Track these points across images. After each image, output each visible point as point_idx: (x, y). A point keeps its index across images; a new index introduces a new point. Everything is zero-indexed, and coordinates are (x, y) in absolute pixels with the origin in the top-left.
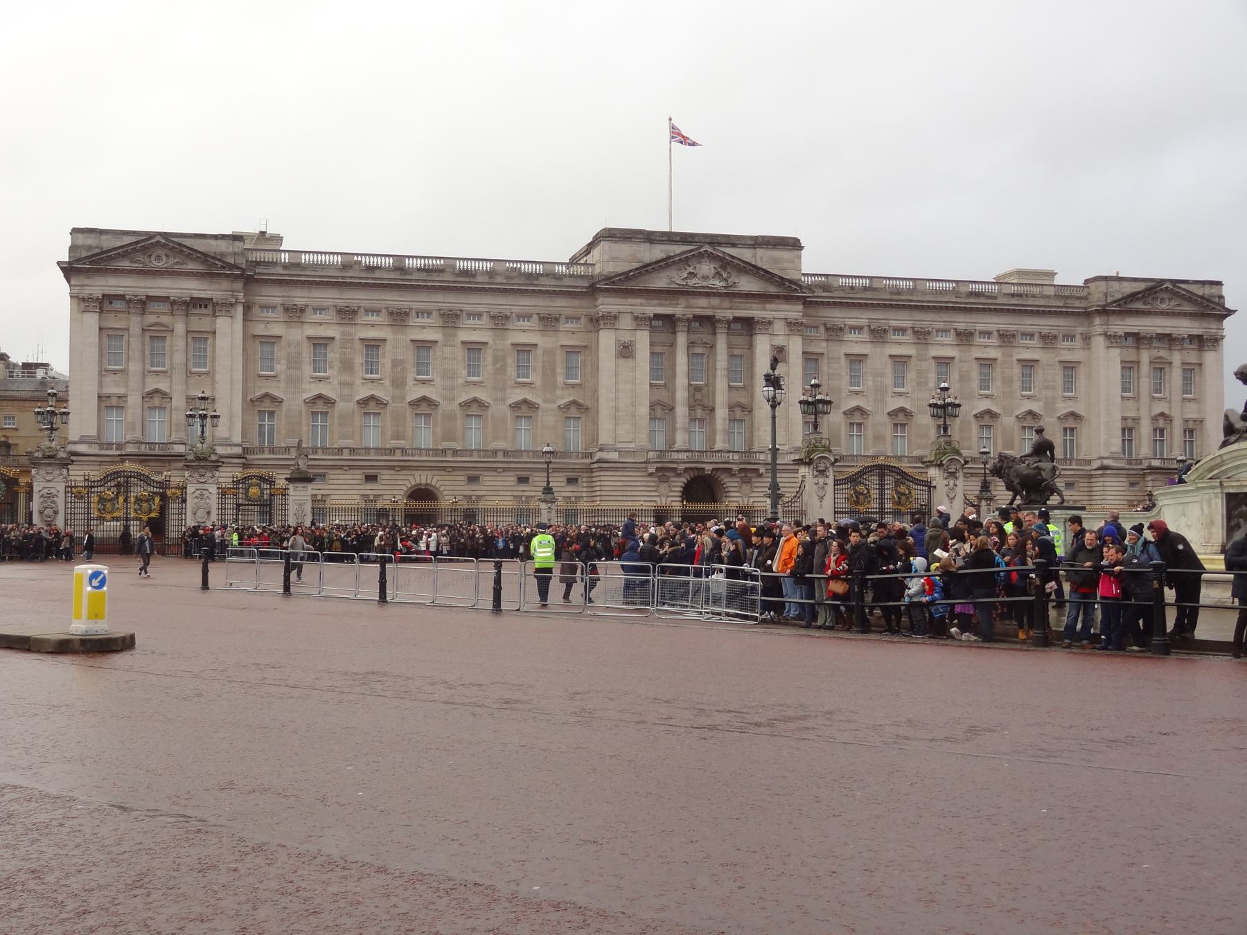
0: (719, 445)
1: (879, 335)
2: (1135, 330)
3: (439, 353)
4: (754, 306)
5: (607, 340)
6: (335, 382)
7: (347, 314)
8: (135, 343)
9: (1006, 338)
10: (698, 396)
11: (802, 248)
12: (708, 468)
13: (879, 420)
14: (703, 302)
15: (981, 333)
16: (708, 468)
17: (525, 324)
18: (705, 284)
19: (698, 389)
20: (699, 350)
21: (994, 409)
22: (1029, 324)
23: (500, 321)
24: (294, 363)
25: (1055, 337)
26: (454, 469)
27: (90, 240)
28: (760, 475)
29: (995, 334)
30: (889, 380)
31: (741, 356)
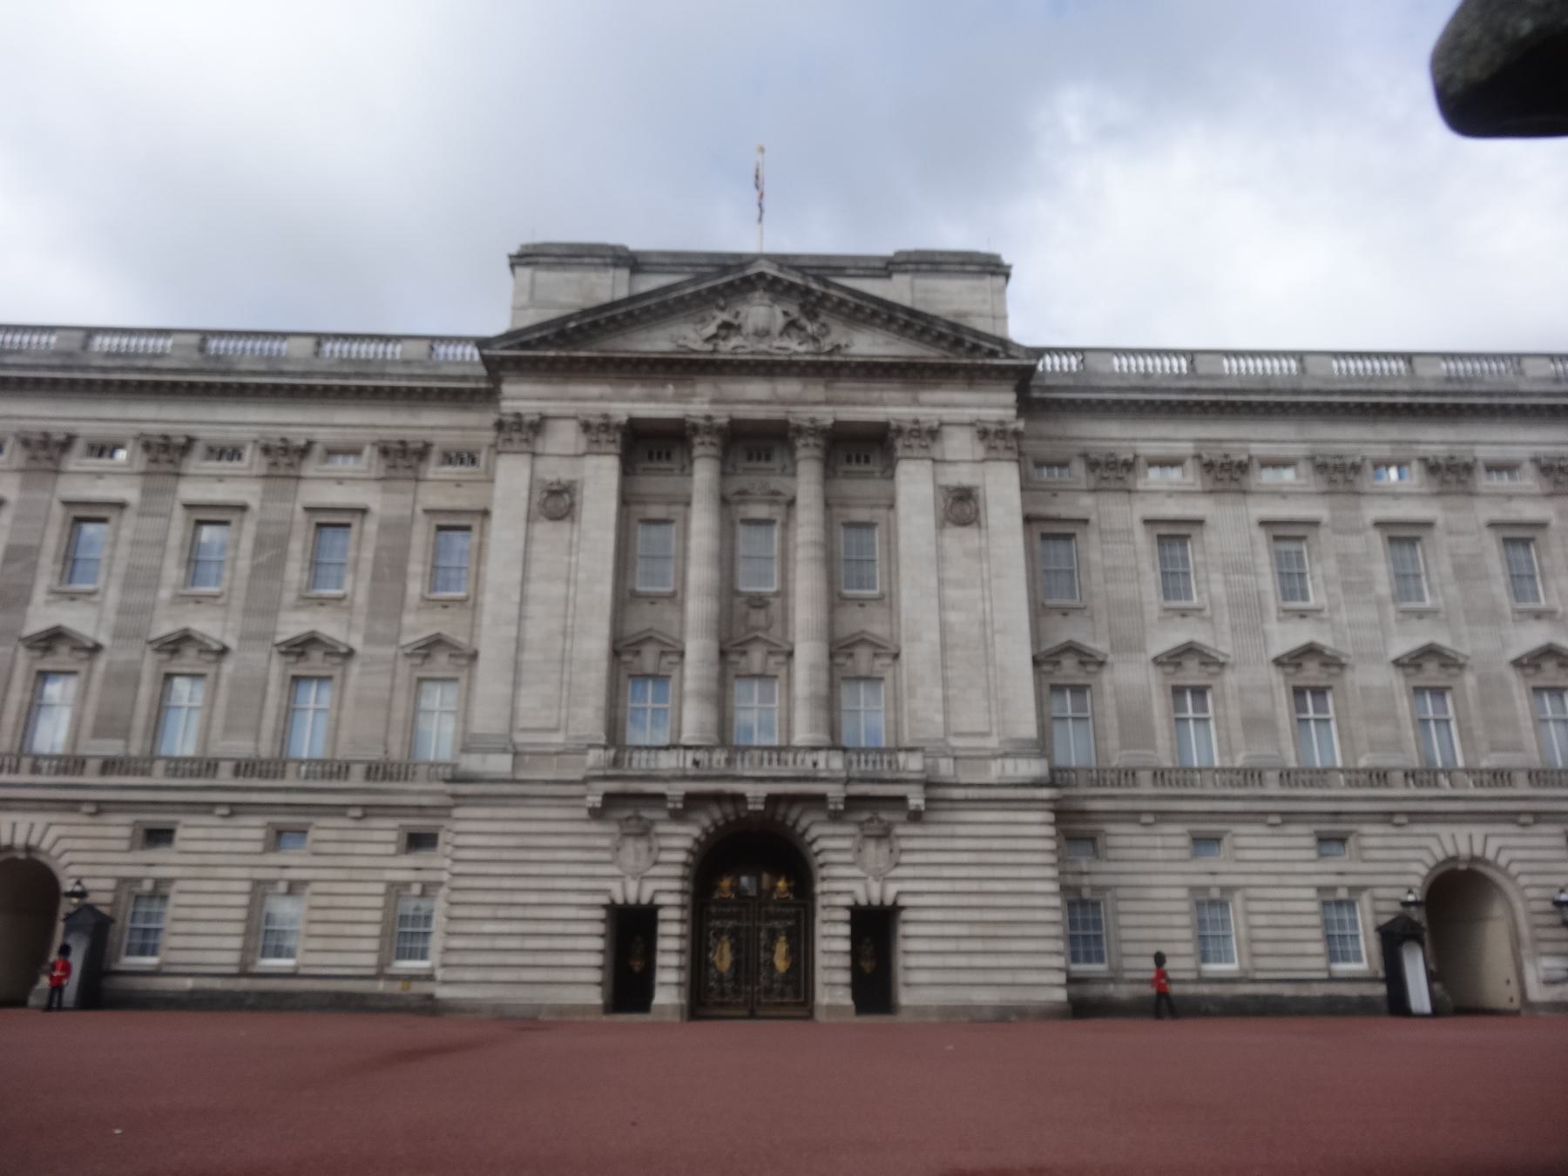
1: (1227, 474)
3: (126, 533)
4: (886, 395)
5: (512, 479)
10: (757, 618)
11: (1007, 276)
12: (755, 792)
13: (1251, 682)
14: (757, 389)
15: (1494, 468)
16: (755, 792)
18: (763, 346)
19: (759, 602)
26: (101, 808)
28: (916, 817)
29: (1528, 468)
30: (1267, 582)
31: (870, 525)
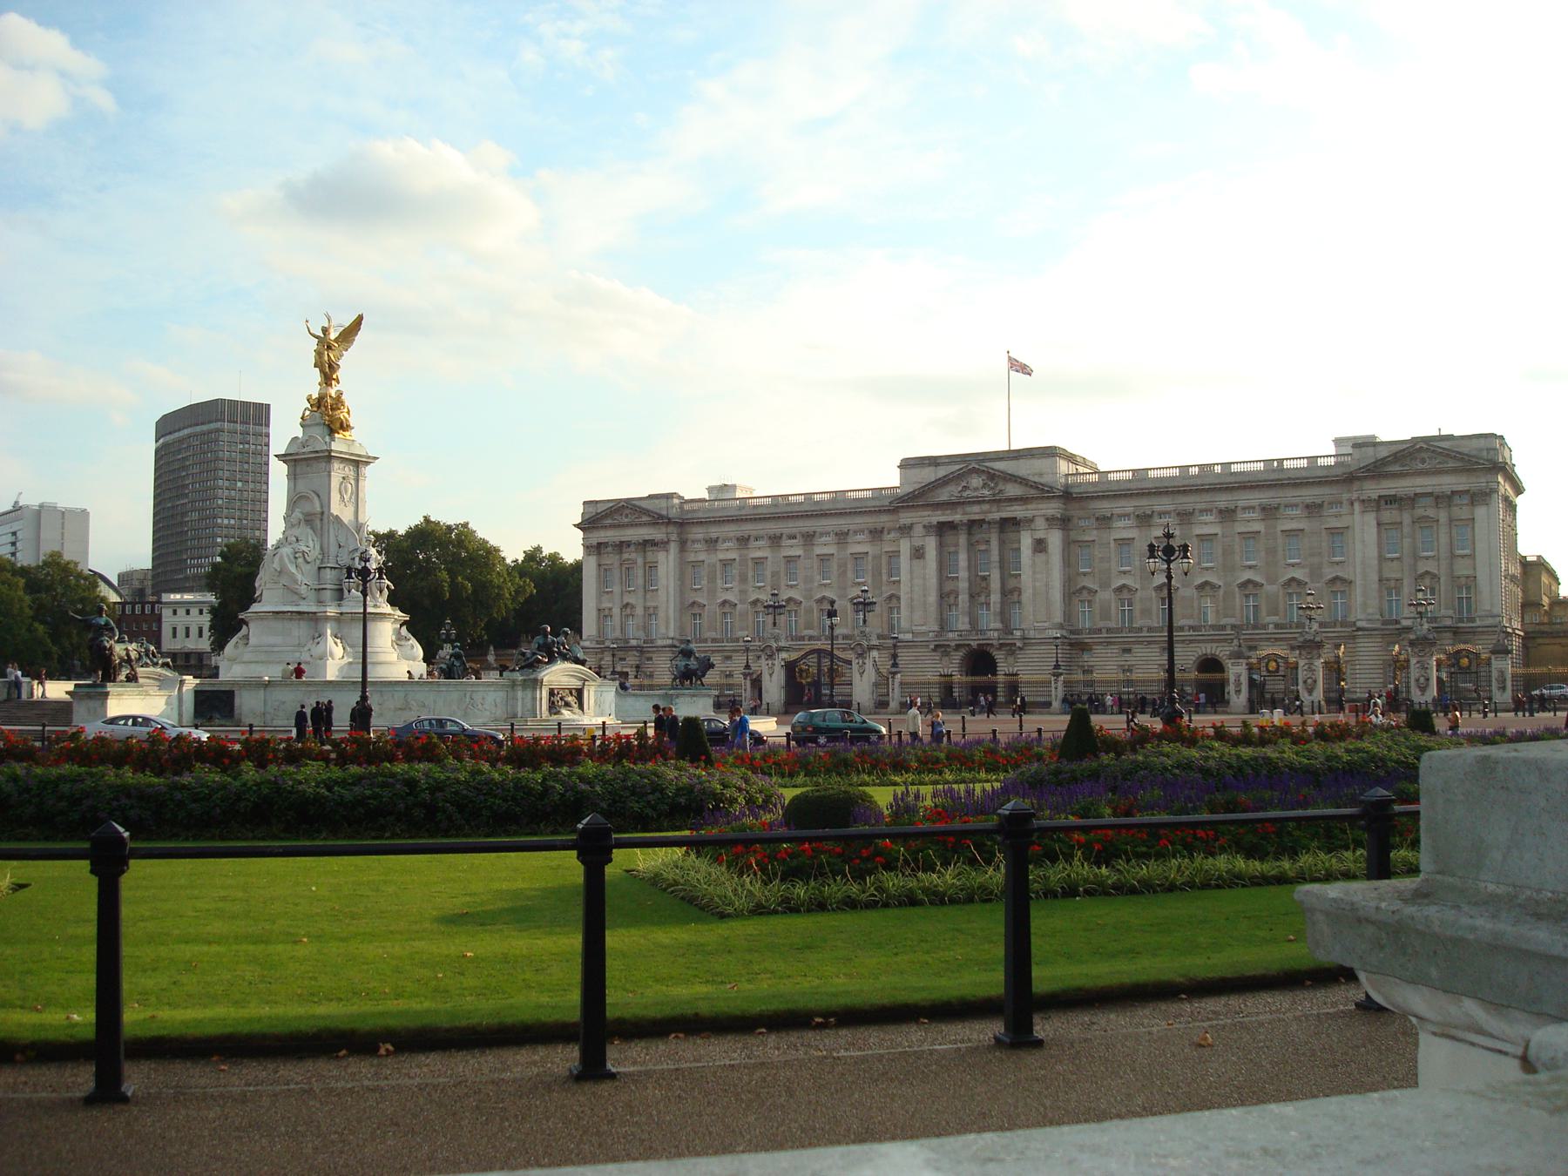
0: (992, 626)
2: (1392, 492)
6: (736, 590)
7: (743, 541)
8: (616, 573)
9: (1269, 512)
14: (976, 508)
15: (1244, 509)
17: (860, 537)
19: (984, 578)
20: (983, 547)
21: (1258, 579)
22: (1290, 495)
23: (842, 537)
24: (712, 579)
25: (1321, 506)
27: (592, 510)
